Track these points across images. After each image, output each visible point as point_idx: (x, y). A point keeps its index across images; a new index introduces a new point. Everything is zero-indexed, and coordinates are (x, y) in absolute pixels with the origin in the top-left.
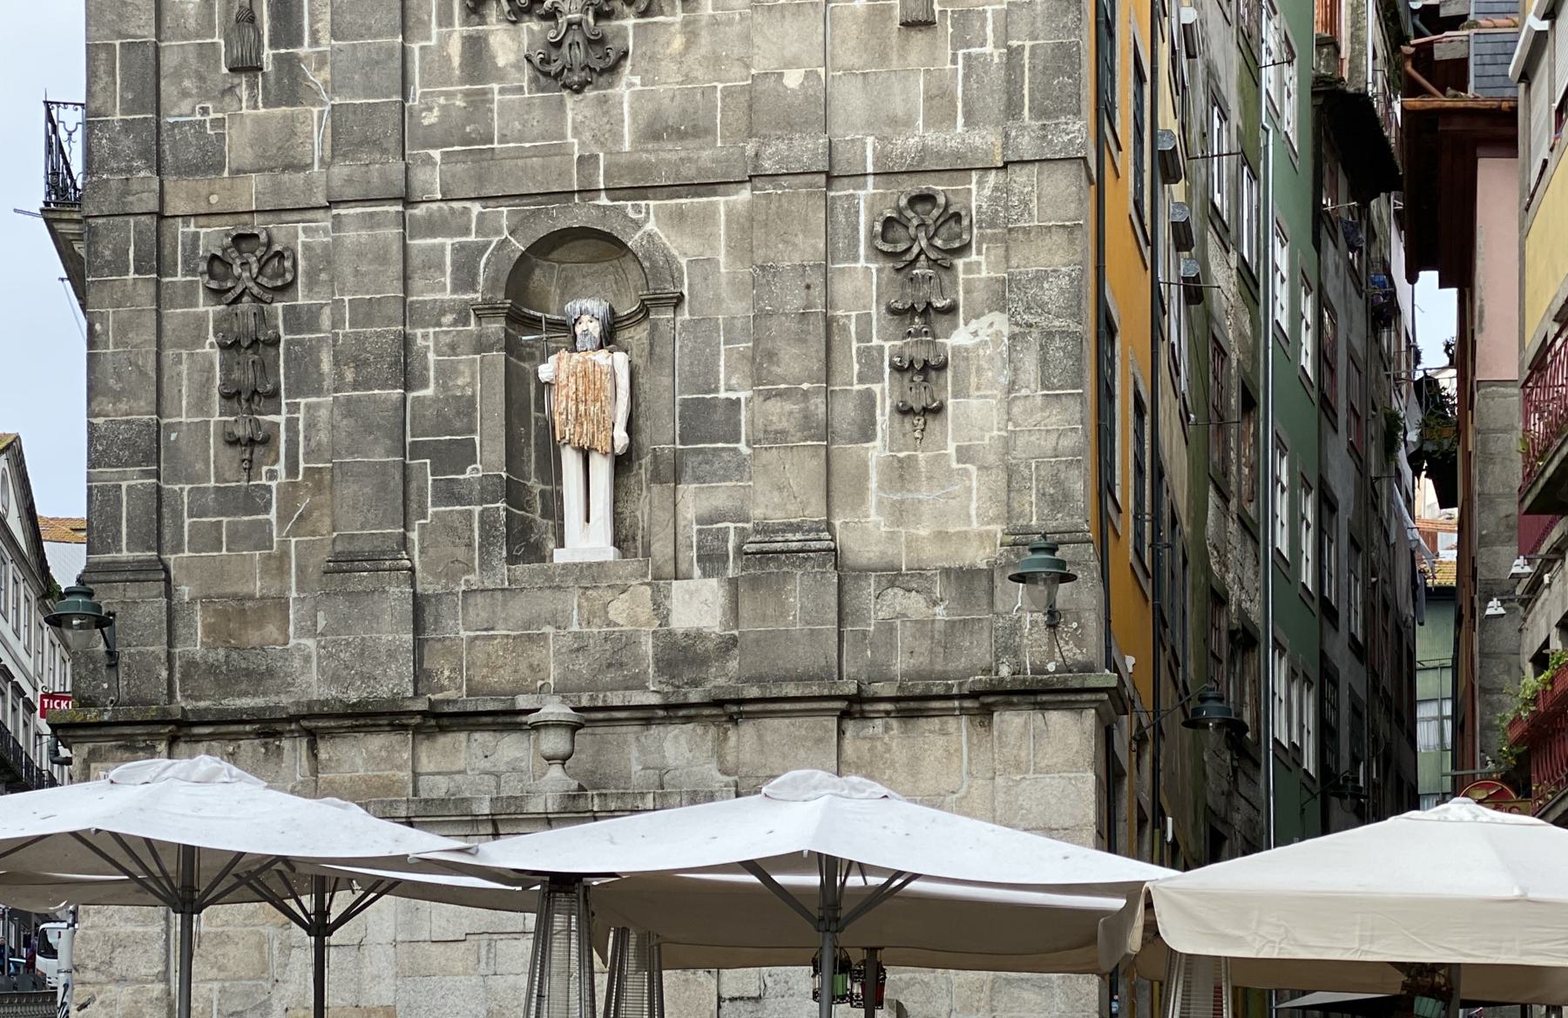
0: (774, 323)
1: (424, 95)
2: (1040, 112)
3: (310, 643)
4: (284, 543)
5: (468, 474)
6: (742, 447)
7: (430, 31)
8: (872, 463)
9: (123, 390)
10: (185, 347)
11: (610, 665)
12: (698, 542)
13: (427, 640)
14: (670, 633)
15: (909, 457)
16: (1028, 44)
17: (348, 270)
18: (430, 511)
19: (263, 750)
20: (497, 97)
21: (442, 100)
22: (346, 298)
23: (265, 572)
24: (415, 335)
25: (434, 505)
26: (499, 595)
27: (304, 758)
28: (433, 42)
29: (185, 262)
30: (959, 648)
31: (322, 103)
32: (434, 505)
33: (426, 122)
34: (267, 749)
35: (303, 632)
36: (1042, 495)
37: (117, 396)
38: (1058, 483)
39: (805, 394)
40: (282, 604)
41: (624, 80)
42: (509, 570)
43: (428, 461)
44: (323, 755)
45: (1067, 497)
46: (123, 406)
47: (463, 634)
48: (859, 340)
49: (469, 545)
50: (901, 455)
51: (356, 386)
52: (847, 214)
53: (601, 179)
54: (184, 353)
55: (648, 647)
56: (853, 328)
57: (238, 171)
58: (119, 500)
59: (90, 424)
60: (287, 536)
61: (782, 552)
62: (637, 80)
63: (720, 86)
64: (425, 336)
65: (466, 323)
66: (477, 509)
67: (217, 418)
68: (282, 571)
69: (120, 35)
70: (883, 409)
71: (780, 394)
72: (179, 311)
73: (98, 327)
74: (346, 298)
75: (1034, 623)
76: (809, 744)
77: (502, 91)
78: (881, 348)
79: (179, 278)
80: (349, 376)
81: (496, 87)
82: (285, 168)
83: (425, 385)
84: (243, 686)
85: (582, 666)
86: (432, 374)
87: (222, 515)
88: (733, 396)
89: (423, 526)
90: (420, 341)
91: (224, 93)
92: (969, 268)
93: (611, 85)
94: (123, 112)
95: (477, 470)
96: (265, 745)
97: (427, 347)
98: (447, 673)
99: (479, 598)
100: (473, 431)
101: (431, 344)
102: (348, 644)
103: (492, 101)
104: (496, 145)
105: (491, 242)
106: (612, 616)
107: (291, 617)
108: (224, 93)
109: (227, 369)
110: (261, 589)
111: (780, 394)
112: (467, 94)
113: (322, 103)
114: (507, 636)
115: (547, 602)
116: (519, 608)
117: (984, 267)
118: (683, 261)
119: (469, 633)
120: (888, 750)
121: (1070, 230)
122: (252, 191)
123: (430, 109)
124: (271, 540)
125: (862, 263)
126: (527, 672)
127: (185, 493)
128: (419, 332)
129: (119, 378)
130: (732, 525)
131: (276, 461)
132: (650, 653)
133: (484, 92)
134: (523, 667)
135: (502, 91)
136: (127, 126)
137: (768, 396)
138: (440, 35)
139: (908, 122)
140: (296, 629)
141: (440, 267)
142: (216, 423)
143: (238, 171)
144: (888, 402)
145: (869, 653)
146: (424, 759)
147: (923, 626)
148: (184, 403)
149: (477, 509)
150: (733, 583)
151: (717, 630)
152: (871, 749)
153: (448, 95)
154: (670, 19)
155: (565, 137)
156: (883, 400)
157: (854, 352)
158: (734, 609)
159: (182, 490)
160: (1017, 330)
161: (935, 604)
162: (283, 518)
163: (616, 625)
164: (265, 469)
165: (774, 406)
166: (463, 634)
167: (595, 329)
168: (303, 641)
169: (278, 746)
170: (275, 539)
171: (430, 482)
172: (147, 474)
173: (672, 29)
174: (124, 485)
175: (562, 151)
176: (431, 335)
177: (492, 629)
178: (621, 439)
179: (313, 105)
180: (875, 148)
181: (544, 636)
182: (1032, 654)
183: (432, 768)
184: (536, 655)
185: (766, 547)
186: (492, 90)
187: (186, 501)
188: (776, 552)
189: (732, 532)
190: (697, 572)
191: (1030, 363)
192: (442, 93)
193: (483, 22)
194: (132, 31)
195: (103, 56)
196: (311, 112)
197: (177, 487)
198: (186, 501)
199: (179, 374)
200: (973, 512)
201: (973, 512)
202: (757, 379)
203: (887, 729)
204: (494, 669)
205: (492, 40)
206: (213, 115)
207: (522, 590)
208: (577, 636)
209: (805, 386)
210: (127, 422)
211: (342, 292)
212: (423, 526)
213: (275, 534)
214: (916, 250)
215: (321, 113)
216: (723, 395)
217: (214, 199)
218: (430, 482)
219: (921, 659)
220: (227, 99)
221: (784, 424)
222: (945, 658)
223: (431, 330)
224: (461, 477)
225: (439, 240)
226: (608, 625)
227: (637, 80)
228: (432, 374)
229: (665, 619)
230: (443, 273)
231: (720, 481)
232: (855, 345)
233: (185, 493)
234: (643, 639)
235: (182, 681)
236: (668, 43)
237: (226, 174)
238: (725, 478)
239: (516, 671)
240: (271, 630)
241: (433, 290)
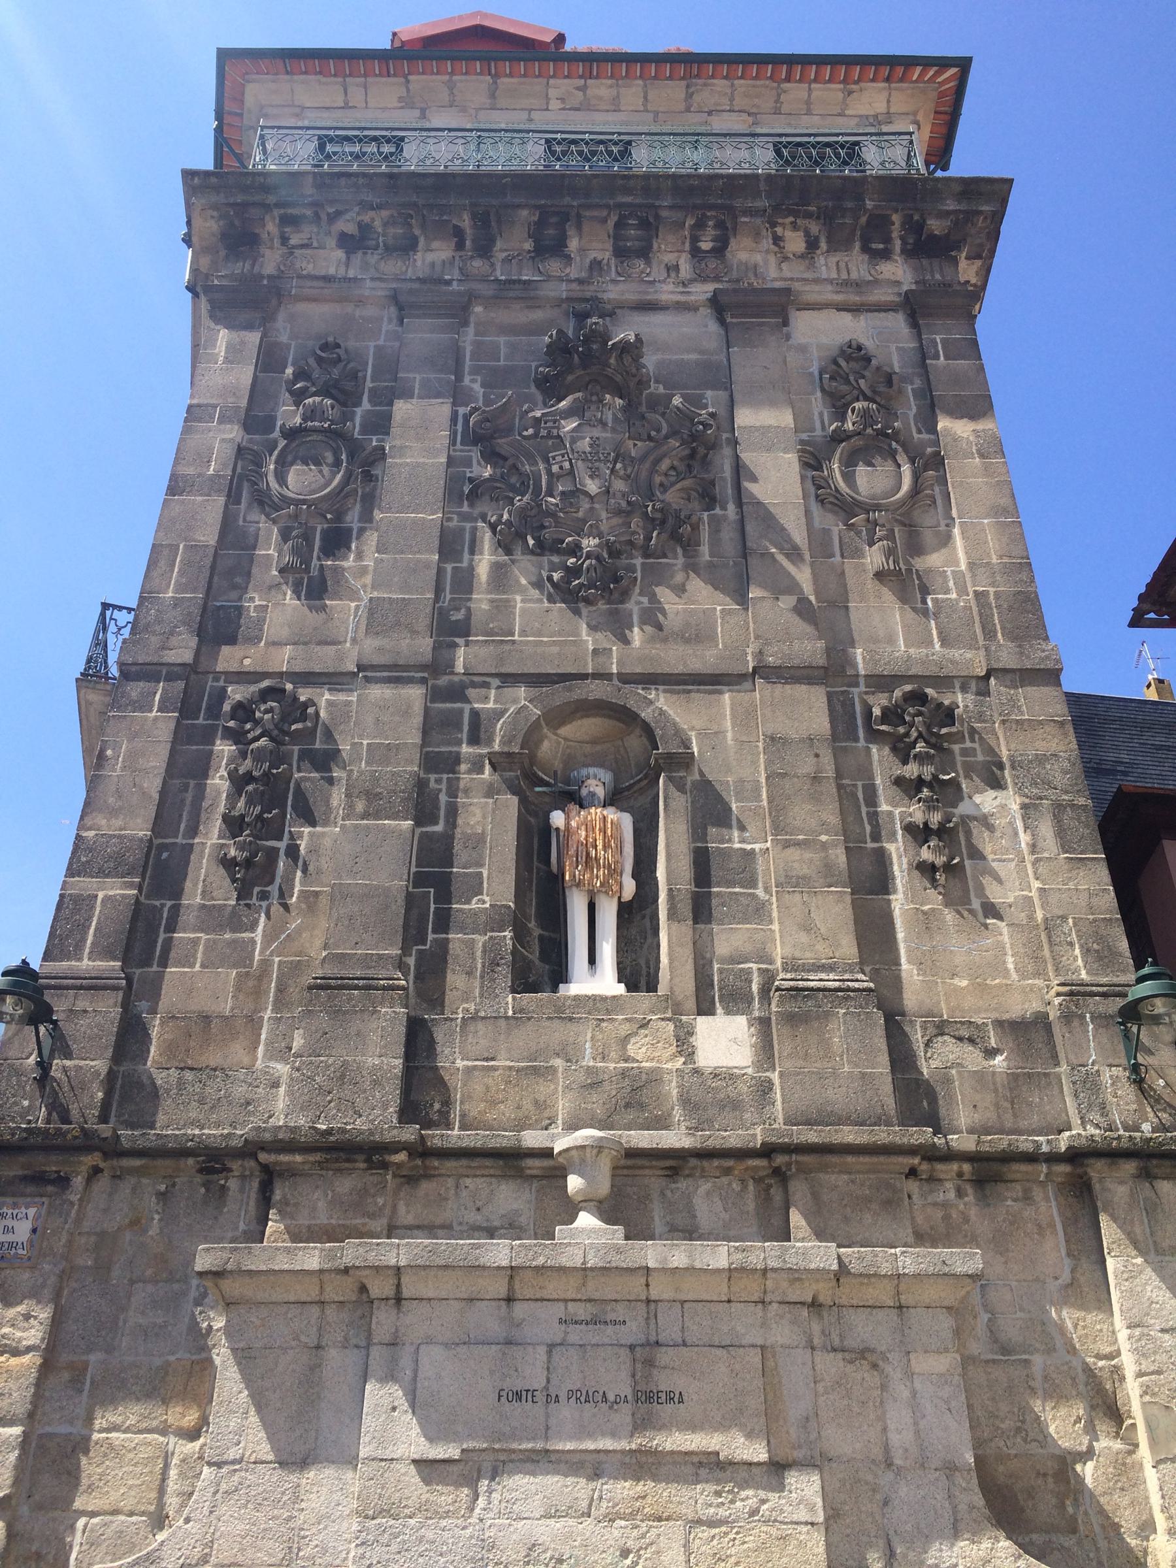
0: (787, 784)
1: (452, 600)
2: (1011, 635)
3: (282, 1069)
4: (266, 964)
5: (474, 905)
6: (760, 892)
7: (462, 557)
8: (897, 913)
9: (121, 808)
10: (194, 777)
11: (628, 1105)
12: (720, 981)
13: (417, 1068)
14: (697, 1071)
15: (933, 910)
16: (991, 590)
17: (370, 720)
18: (431, 937)
19: (203, 1190)
22: (365, 742)
23: (238, 988)
24: (428, 780)
25: (434, 932)
26: (502, 1023)
27: (252, 1203)
29: (208, 709)
30: (1030, 1104)
31: (359, 599)
32: (434, 932)
33: (453, 618)
34: (207, 1190)
35: (271, 1055)
36: (1086, 951)
37: (113, 813)
38: (1100, 939)
39: (824, 846)
40: (254, 1023)
42: (514, 999)
43: (432, 890)
44: (277, 1196)
45: (1114, 954)
46: (119, 822)
47: (460, 1064)
48: (867, 805)
49: (470, 973)
50: (926, 908)
51: (363, 817)
52: (843, 704)
53: (614, 666)
54: (192, 783)
55: (672, 1089)
56: (860, 795)
57: (274, 644)
58: (93, 907)
59: (78, 837)
60: (271, 954)
61: (819, 990)
62: (645, 600)
63: (719, 608)
64: (438, 781)
65: (481, 771)
66: (480, 940)
67: (215, 841)
68: (258, 993)
69: (185, 539)
70: (900, 866)
71: (798, 844)
72: (194, 747)
73: (109, 752)
74: (365, 742)
75: (1115, 1080)
76: (874, 1206)
78: (890, 813)
79: (201, 721)
80: (360, 806)
81: (518, 598)
82: (320, 643)
83: (436, 823)
84: (193, 1115)
85: (597, 1103)
86: (442, 813)
87: (202, 931)
88: (749, 847)
89: (420, 952)
90: (432, 784)
91: (270, 588)
92: (965, 752)
94: (176, 591)
95: (484, 902)
96: (206, 1185)
97: (440, 790)
98: (437, 1106)
99: (480, 1025)
100: (482, 866)
101: (444, 786)
102: (328, 1067)
103: (515, 607)
104: (516, 638)
105: (506, 710)
106: (631, 1049)
107: (263, 1037)
108: (270, 588)
109: (232, 799)
110: (232, 1009)
111: (798, 844)
112: (492, 601)
113: (359, 599)
114: (510, 1068)
115: (558, 1033)
116: (524, 1037)
117: (979, 752)
118: (693, 735)
119: (466, 1063)
120: (967, 1220)
121: (1062, 724)
122: (284, 659)
123: (458, 609)
124: (252, 959)
125: (862, 743)
126: (531, 1107)
127: (166, 910)
128: (433, 777)
129: (119, 794)
130: (754, 966)
131: (271, 882)
132: (675, 1092)
133: (508, 601)
134: (528, 1105)
135: (522, 601)
136: (177, 602)
137: (787, 845)
139: (891, 640)
140: (267, 1050)
141: (458, 727)
142: (213, 845)
143: (274, 644)
144: (905, 860)
145: (925, 1103)
146: (402, 1208)
147: (981, 1078)
148: (183, 826)
149: (480, 940)
150: (763, 1025)
151: (750, 1071)
152: (947, 1218)
154: (674, 561)
155: (578, 635)
156: (900, 857)
157: (864, 815)
158: (765, 1051)
159: (163, 905)
160: (1027, 801)
161: (991, 1053)
162: (269, 938)
163: (635, 1061)
164: (256, 890)
165: (794, 854)
166: (460, 1064)
167: (600, 792)
168: (272, 1064)
169: (223, 1186)
170: (257, 957)
171: (432, 910)
172: (131, 885)
174: (101, 895)
175: (578, 643)
176: (445, 781)
177: (493, 1059)
178: (629, 887)
179: (352, 600)
180: (864, 658)
181: (553, 1070)
182: (1120, 1114)
183: (409, 1219)
184: (542, 1089)
185: (801, 984)
187: (165, 915)
188: (812, 989)
189: (755, 975)
190: (719, 1010)
191: (1046, 829)
194: (197, 537)
195: (166, 552)
196: (350, 607)
197: (157, 903)
198: (165, 915)
199: (183, 801)
200: (1011, 966)
201: (1011, 966)
202: (777, 829)
203: (960, 1193)
204: (493, 1103)
206: (257, 603)
207: (529, 1019)
208: (589, 1071)
209: (824, 838)
210: (120, 837)
211: (361, 737)
212: (420, 952)
213: (257, 953)
214: (914, 734)
215: (357, 607)
216: (737, 846)
217: (247, 662)
218: (432, 910)
219: (989, 1115)
220: (273, 592)
221: (806, 871)
222: (1015, 1116)
223: (445, 776)
224: (466, 907)
225: (458, 705)
226: (626, 1061)
227: (645, 600)
228: (442, 813)
229: (691, 1055)
230: (462, 731)
231: (739, 923)
232: (864, 810)
233: (166, 910)
234: (666, 1077)
235: (120, 1105)
236: (672, 577)
237: (262, 644)
238: (746, 920)
239: (519, 1107)
240: (237, 1052)
241: (449, 744)
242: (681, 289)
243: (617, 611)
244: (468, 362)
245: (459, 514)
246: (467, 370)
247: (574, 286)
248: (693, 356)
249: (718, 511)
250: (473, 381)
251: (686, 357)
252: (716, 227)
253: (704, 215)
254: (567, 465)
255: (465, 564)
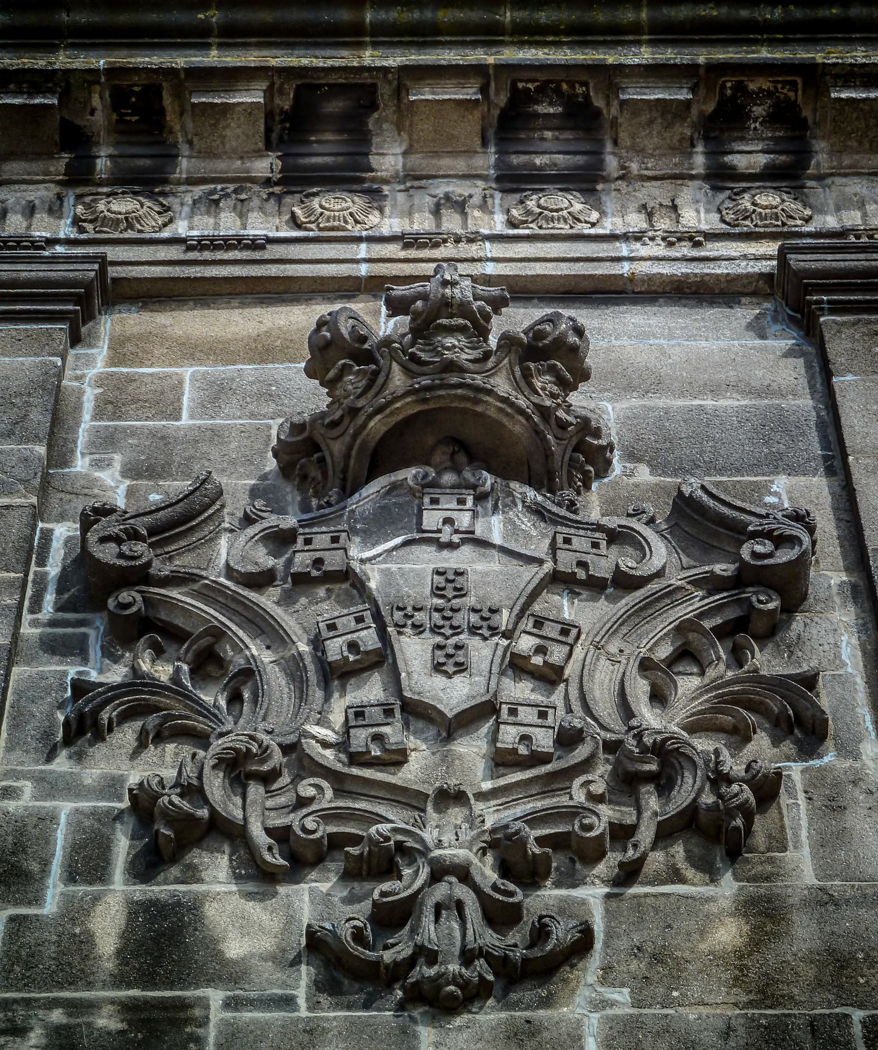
7: (42, 889)
20: (217, 1014)
21: (57, 1016)
28: (50, 906)
41: (583, 994)
62: (622, 996)
63: (858, 1015)
77: (232, 1004)
81: (216, 996)
93: (546, 1002)
103: (204, 1022)
112: (128, 1008)
135: (232, 1004)
138: (68, 900)
153: (74, 1007)
173: (713, 908)
186: (204, 1004)
192: (53, 1004)
193: (192, 875)
205: (211, 911)
242: (685, 249)
243: (532, 1029)
244: (86, 423)
245: (40, 779)
246: (82, 438)
247: (392, 250)
248: (730, 402)
249: (829, 758)
250: (98, 464)
251: (709, 403)
252: (771, 120)
253: (740, 88)
254: (369, 638)
255: (50, 906)
